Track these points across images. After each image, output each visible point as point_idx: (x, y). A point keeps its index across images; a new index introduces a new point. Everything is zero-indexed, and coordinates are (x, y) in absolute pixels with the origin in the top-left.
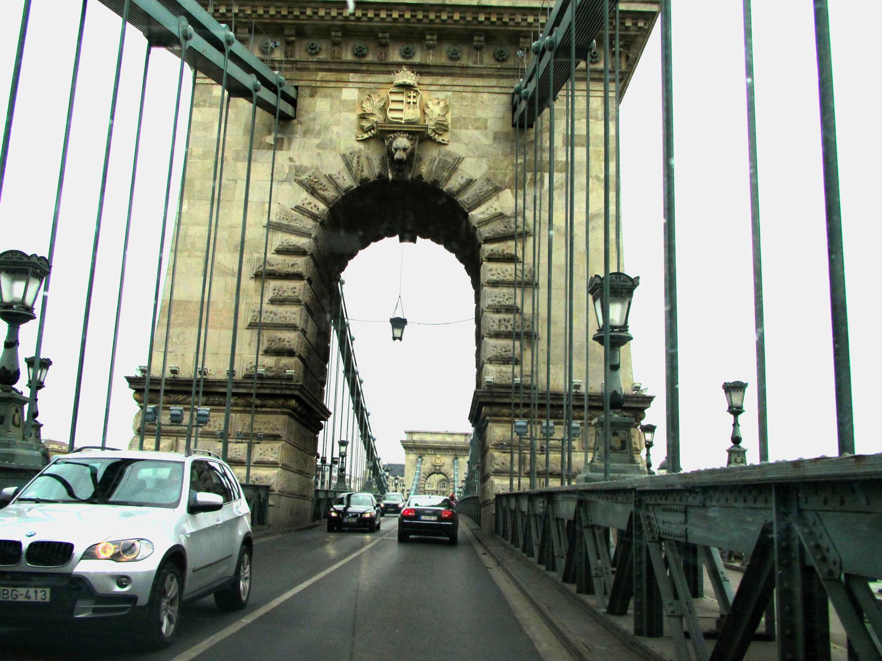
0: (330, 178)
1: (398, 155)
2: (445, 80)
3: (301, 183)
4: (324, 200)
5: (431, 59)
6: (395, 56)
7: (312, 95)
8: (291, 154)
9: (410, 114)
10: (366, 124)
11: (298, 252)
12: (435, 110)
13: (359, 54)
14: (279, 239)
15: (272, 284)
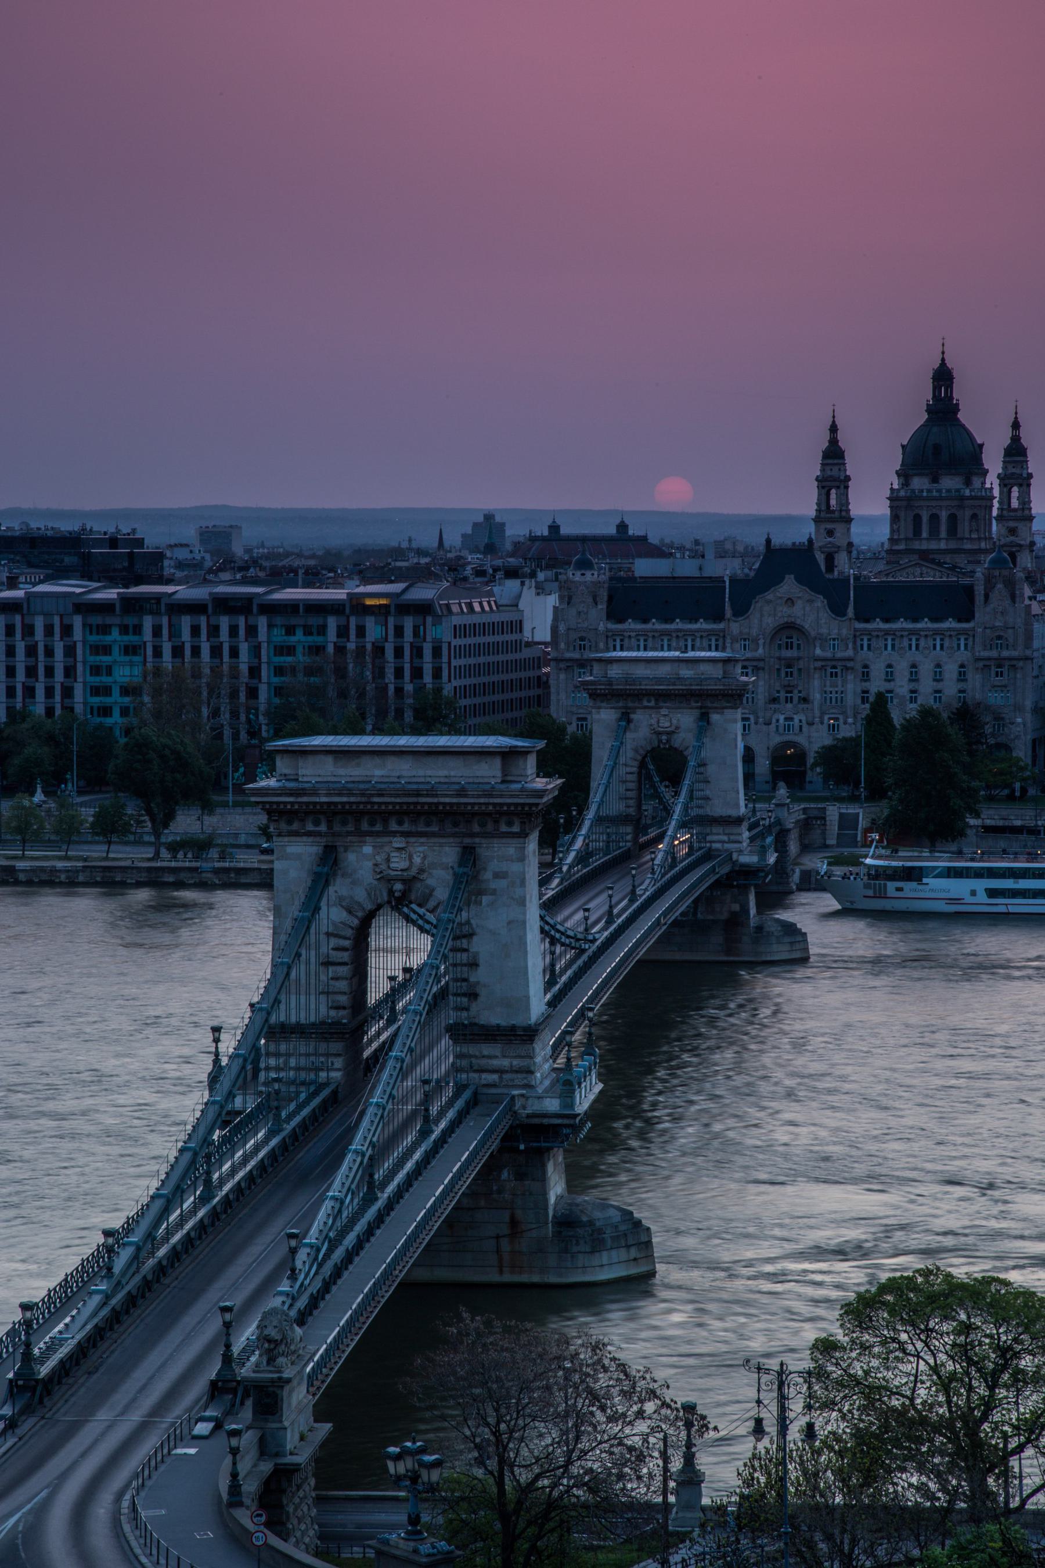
0: (359, 904)
1: (396, 894)
2: (423, 840)
3: (342, 906)
4: (356, 917)
5: (413, 829)
6: (394, 826)
7: (345, 851)
8: (335, 888)
9: (404, 865)
10: (378, 870)
11: (344, 949)
12: (417, 860)
13: (372, 824)
14: (334, 942)
15: (331, 969)
